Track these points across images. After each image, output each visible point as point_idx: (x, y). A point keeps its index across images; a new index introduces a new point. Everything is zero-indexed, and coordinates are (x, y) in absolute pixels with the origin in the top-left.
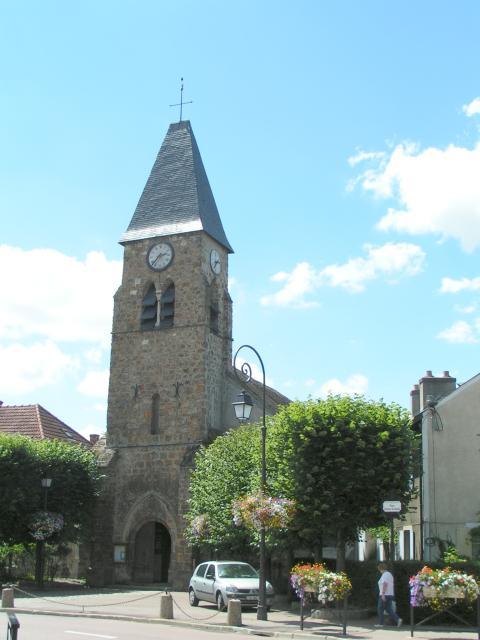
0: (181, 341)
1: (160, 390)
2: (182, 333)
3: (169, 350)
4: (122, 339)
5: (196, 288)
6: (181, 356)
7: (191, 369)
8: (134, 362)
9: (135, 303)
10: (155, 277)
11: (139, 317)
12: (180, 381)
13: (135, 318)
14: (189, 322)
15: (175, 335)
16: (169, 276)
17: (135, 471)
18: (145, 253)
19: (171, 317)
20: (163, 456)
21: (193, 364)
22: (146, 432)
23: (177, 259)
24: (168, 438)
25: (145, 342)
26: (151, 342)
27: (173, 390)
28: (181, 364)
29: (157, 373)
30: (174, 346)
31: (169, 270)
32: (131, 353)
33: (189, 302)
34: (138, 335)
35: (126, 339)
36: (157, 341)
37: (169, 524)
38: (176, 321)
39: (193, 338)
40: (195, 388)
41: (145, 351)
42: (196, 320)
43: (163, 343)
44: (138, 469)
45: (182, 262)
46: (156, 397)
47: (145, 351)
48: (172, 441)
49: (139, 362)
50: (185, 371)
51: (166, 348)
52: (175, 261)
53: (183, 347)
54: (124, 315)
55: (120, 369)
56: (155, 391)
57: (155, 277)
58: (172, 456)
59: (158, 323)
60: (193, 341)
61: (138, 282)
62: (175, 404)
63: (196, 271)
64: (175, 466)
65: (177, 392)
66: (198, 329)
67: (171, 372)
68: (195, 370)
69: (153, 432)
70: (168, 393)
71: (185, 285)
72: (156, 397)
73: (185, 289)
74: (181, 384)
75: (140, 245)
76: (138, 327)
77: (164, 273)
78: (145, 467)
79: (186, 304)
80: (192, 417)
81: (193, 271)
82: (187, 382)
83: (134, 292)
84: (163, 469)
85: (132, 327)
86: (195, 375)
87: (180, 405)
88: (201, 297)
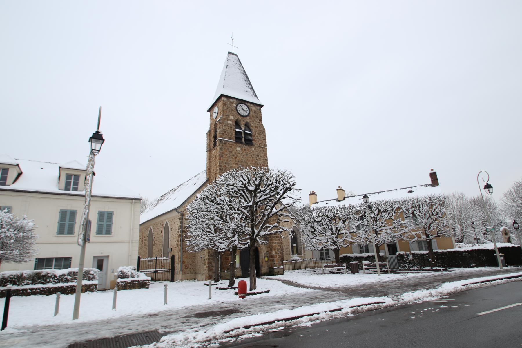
3: (251, 156)
6: (258, 160)
8: (234, 157)
9: (231, 128)
10: (241, 118)
13: (232, 134)
14: (260, 145)
15: (253, 149)
16: (248, 121)
23: (252, 114)
25: (239, 149)
26: (242, 150)
31: (248, 118)
32: (231, 152)
33: (259, 136)
34: (234, 144)
39: (262, 153)
41: (239, 153)
47: (239, 153)
49: (236, 158)
51: (250, 155)
52: (250, 115)
53: (258, 156)
54: (225, 132)
55: (226, 159)
61: (232, 117)
63: (261, 123)
75: (231, 100)
77: (245, 119)
81: (259, 123)
83: (230, 122)
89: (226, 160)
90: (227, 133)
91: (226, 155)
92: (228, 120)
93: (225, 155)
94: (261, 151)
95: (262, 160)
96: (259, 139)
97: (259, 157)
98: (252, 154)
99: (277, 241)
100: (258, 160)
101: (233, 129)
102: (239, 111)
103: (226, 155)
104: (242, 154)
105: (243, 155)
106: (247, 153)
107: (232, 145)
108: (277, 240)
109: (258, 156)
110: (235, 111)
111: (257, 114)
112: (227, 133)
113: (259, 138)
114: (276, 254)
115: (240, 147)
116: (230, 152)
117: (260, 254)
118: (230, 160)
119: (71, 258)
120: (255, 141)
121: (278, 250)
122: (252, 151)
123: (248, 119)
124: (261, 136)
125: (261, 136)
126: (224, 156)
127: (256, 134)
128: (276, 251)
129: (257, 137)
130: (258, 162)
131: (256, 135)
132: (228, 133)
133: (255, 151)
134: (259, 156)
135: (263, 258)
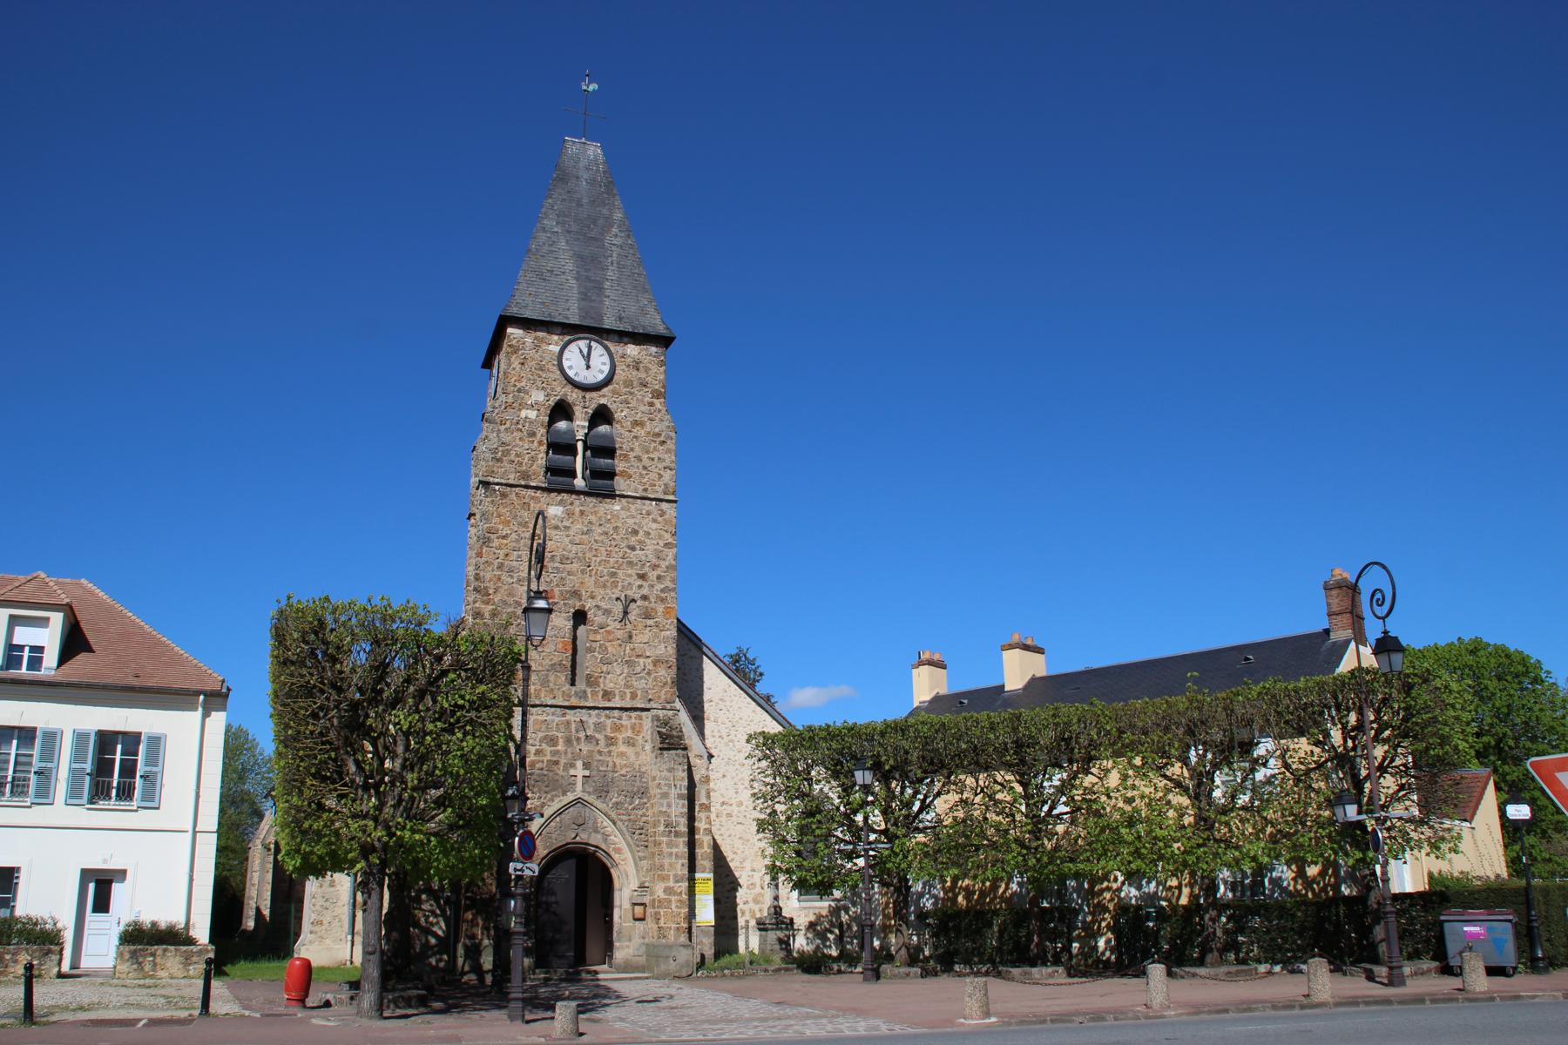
0: (630, 521)
1: (589, 605)
2: (633, 507)
4: (504, 495)
5: (659, 435)
6: (633, 548)
7: (653, 575)
9: (533, 434)
10: (573, 396)
11: (541, 460)
12: (629, 593)
13: (533, 459)
15: (617, 507)
16: (603, 401)
17: (538, 752)
18: (557, 349)
19: (610, 475)
20: (599, 727)
21: (655, 567)
22: (563, 678)
23: (621, 374)
24: (607, 695)
26: (570, 514)
27: (618, 609)
28: (630, 563)
29: (583, 572)
30: (616, 528)
31: (605, 390)
35: (513, 496)
36: (582, 513)
37: (616, 856)
38: (620, 484)
39: (655, 521)
40: (660, 608)
42: (660, 489)
43: (593, 518)
44: (547, 749)
45: (628, 383)
46: (580, 617)
47: (557, 528)
48: (617, 703)
50: (642, 577)
53: (635, 532)
55: (502, 553)
56: (578, 605)
57: (573, 396)
58: (617, 728)
59: (579, 482)
60: (654, 526)
61: (538, 396)
62: (620, 634)
64: (623, 748)
65: (626, 613)
66: (664, 506)
67: (613, 575)
68: (659, 577)
69: (573, 683)
70: (607, 612)
71: (636, 423)
72: (580, 617)
73: (638, 431)
74: (634, 601)
76: (539, 480)
77: (594, 394)
78: (560, 747)
79: (639, 459)
80: (656, 663)
82: (645, 598)
83: (532, 414)
84: (600, 752)
85: (525, 475)
86: (659, 587)
87: (630, 637)
88: (668, 451)
89: (501, 557)
90: (512, 457)
91: (504, 537)
92: (523, 406)
93: (498, 538)
94: (649, 513)
95: (650, 547)
96: (645, 468)
97: (641, 536)
98: (609, 528)
99: (674, 850)
100: (633, 548)
101: (539, 435)
102: (570, 367)
103: (504, 537)
104: (567, 528)
105: (571, 533)
106: (590, 523)
107: (532, 498)
108: (677, 846)
109: (635, 532)
110: (555, 369)
111: (647, 370)
112: (512, 457)
113: (646, 462)
114: (670, 894)
115: (561, 503)
116: (520, 524)
117: (617, 895)
118: (520, 556)
119: (18, 869)
120: (625, 475)
121: (677, 882)
122: (613, 516)
123: (604, 396)
124: (655, 455)
125: (655, 455)
126: (496, 543)
127: (632, 449)
128: (671, 884)
129: (639, 459)
130: (632, 555)
131: (632, 454)
132: (517, 455)
133: (623, 514)
134: (641, 533)
135: (627, 905)
